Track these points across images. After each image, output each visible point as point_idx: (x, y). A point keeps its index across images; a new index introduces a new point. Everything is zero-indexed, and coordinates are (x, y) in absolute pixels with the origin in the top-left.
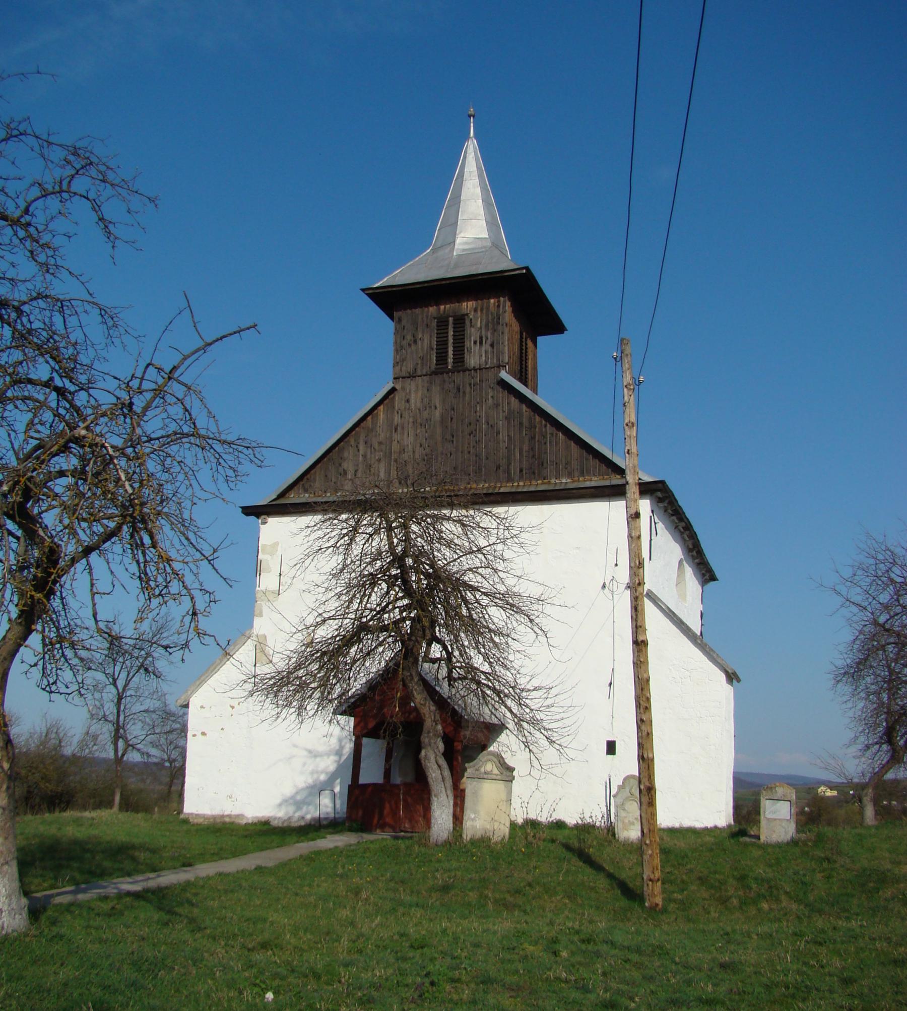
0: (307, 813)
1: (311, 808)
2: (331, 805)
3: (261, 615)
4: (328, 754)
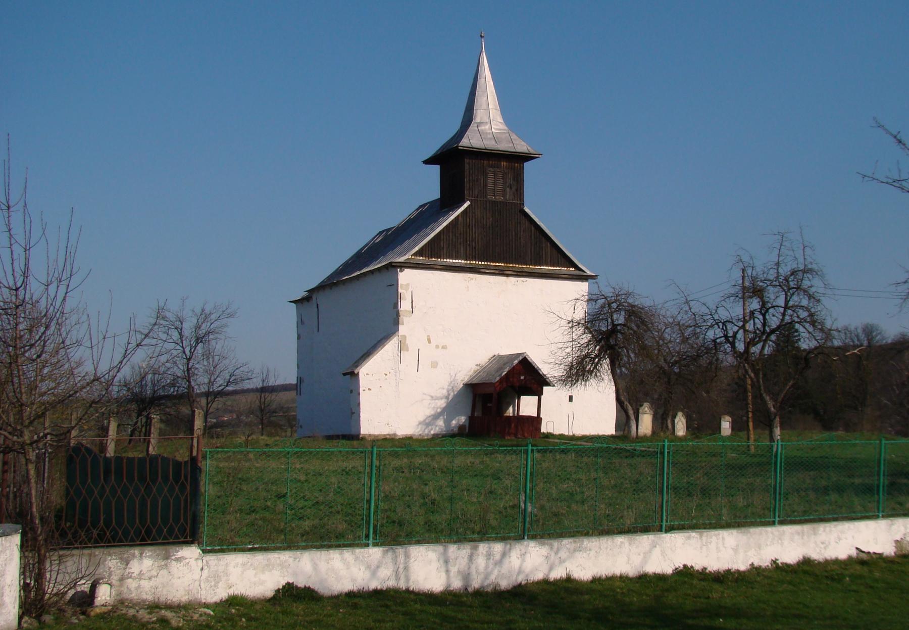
0: (432, 429)
1: (434, 427)
2: (443, 425)
3: (403, 324)
4: (442, 399)
